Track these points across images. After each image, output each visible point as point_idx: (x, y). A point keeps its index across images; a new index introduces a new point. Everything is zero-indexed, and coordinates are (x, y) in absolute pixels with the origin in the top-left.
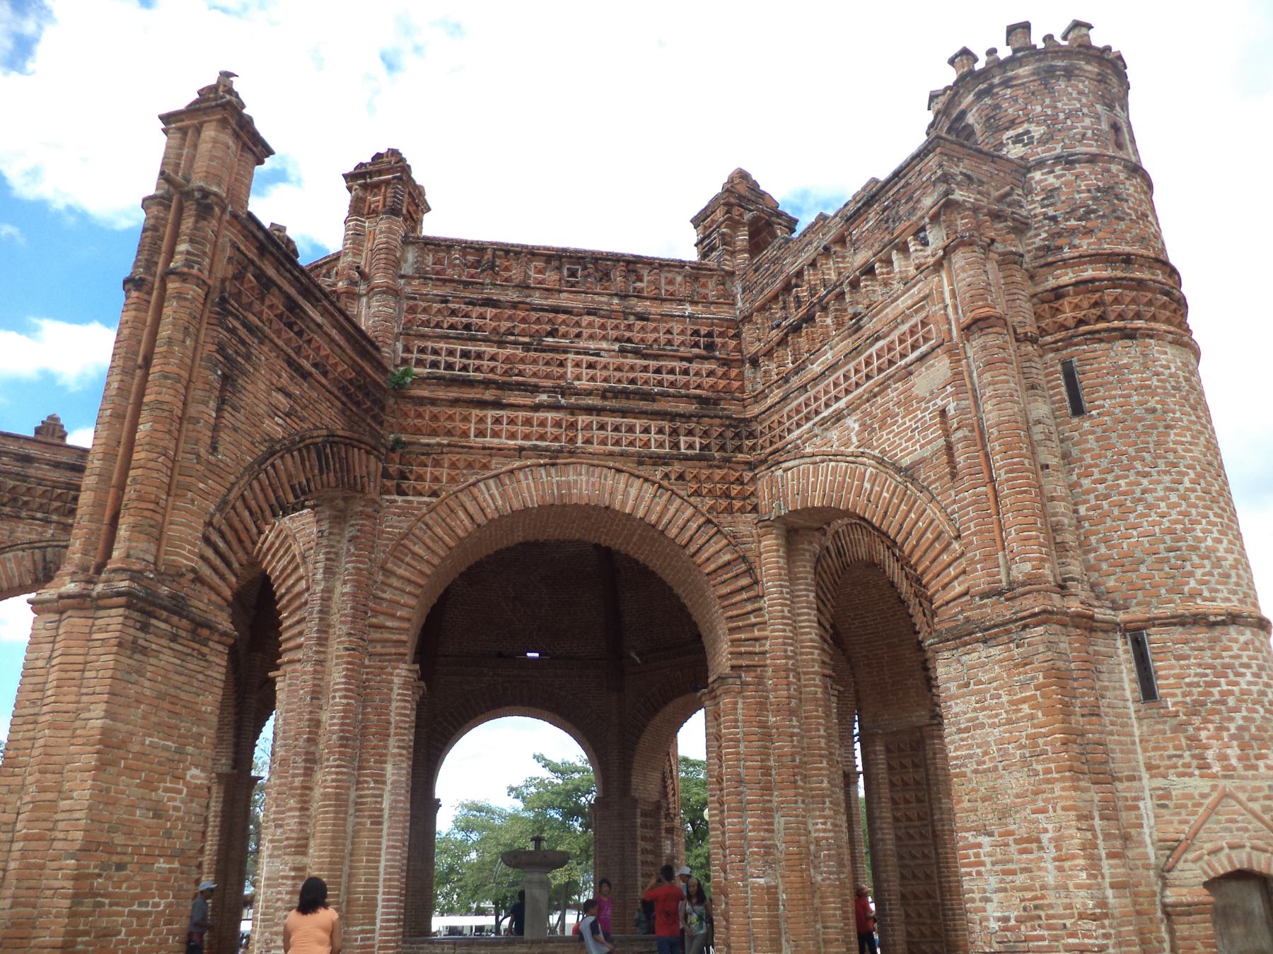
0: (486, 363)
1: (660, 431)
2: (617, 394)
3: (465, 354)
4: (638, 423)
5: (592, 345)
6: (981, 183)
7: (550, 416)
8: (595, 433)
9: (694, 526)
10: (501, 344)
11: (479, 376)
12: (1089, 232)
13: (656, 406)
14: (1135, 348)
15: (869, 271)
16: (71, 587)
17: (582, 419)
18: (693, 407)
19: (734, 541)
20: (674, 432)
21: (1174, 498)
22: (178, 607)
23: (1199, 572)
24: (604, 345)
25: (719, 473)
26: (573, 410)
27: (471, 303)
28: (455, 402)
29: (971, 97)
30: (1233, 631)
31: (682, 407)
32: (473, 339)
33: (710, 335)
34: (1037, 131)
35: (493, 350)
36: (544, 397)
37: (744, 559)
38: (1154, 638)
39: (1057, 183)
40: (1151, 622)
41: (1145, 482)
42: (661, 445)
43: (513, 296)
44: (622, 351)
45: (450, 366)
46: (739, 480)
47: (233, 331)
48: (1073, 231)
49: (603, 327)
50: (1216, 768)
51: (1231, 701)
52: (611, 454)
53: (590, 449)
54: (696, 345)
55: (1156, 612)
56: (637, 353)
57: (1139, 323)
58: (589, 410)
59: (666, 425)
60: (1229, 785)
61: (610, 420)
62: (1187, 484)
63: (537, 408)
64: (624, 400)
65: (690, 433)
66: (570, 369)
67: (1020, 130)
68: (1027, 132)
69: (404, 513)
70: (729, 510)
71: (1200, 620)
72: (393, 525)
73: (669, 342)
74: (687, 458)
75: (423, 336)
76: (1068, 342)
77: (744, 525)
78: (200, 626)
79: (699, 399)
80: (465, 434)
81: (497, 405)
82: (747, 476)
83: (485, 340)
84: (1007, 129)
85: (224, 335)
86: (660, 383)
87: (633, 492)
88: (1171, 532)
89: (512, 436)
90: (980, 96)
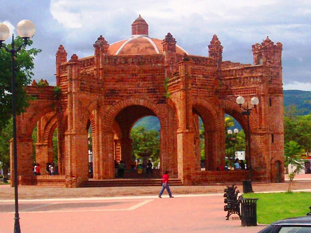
15: (247, 78)
17: (199, 89)
29: (263, 51)
39: (273, 71)
40: (275, 133)
44: (203, 77)
66: (197, 80)
67: (269, 60)
68: (270, 61)
74: (210, 96)
84: (268, 59)
90: (264, 52)
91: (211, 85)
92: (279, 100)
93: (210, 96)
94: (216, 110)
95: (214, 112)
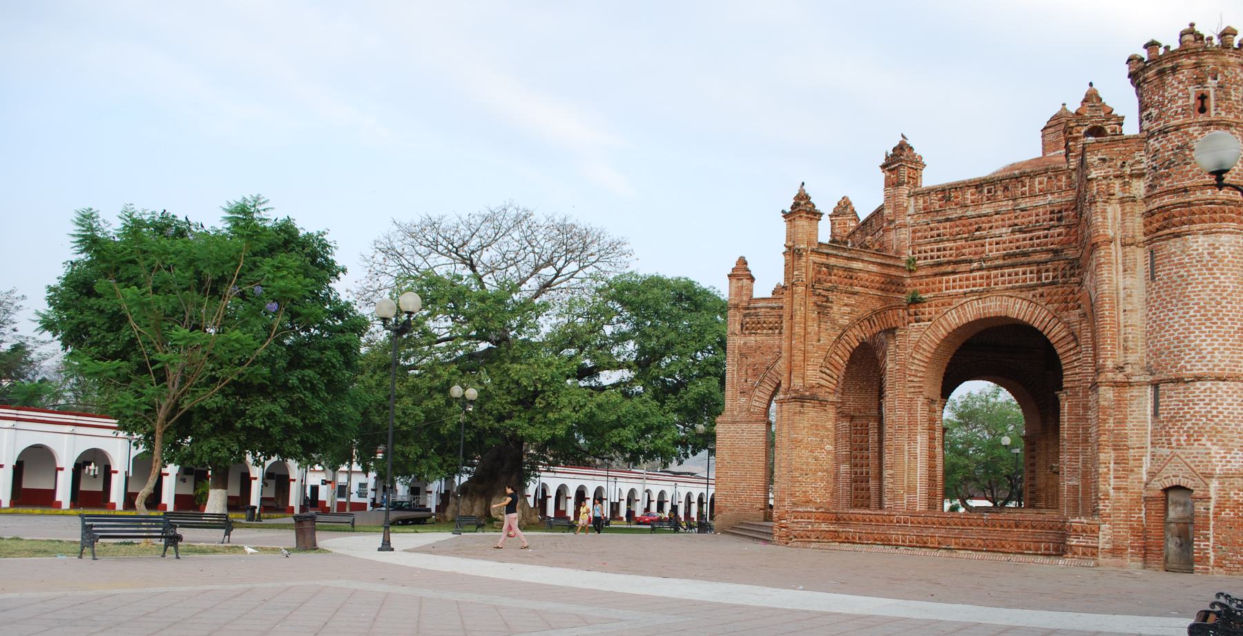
0: (948, 252)
1: (1031, 272)
2: (1010, 256)
3: (938, 250)
4: (1020, 270)
5: (997, 232)
6: (1112, 160)
7: (977, 274)
8: (1001, 279)
9: (1047, 320)
10: (955, 241)
11: (946, 259)
12: (1169, 176)
13: (1030, 259)
14: (1178, 242)
16: (782, 396)
17: (993, 272)
18: (1050, 256)
19: (1068, 325)
20: (1039, 272)
21: (1183, 321)
22: (813, 398)
23: (1187, 358)
24: (1004, 230)
25: (1060, 290)
26: (989, 269)
27: (939, 222)
28: (935, 275)
30: (1198, 384)
31: (1044, 257)
32: (942, 241)
33: (1060, 212)
34: (1154, 112)
35: (952, 244)
36: (975, 265)
37: (1073, 334)
38: (1161, 387)
40: (1161, 381)
41: (1171, 314)
42: (1031, 280)
43: (959, 212)
45: (932, 258)
46: (1072, 292)
47: (819, 294)
48: (1162, 175)
49: (1003, 220)
50: (1174, 445)
51: (1188, 416)
52: (1007, 289)
53: (997, 288)
54: (1051, 220)
55: (1163, 377)
56: (1021, 231)
57: (1185, 228)
58: (996, 268)
59: (1034, 268)
60: (1178, 452)
61: (1007, 271)
62: (1192, 313)
63: (971, 271)
64: (1014, 258)
65: (1047, 271)
66: (987, 247)
69: (919, 330)
70: (1066, 309)
71: (1178, 380)
72: (914, 336)
73: (1037, 221)
74: (1044, 285)
75: (920, 245)
76: (1151, 241)
77: (1074, 316)
78: (822, 403)
79: (1052, 250)
80: (940, 290)
81: (954, 273)
82: (1076, 289)
83: (948, 240)
85: (815, 299)
86: (1032, 246)
87: (1018, 306)
88: (1178, 338)
89: (961, 287)
91: (1047, 251)
92: (1183, 252)
93: (1044, 285)
94: (1068, 325)
95: (1056, 333)
